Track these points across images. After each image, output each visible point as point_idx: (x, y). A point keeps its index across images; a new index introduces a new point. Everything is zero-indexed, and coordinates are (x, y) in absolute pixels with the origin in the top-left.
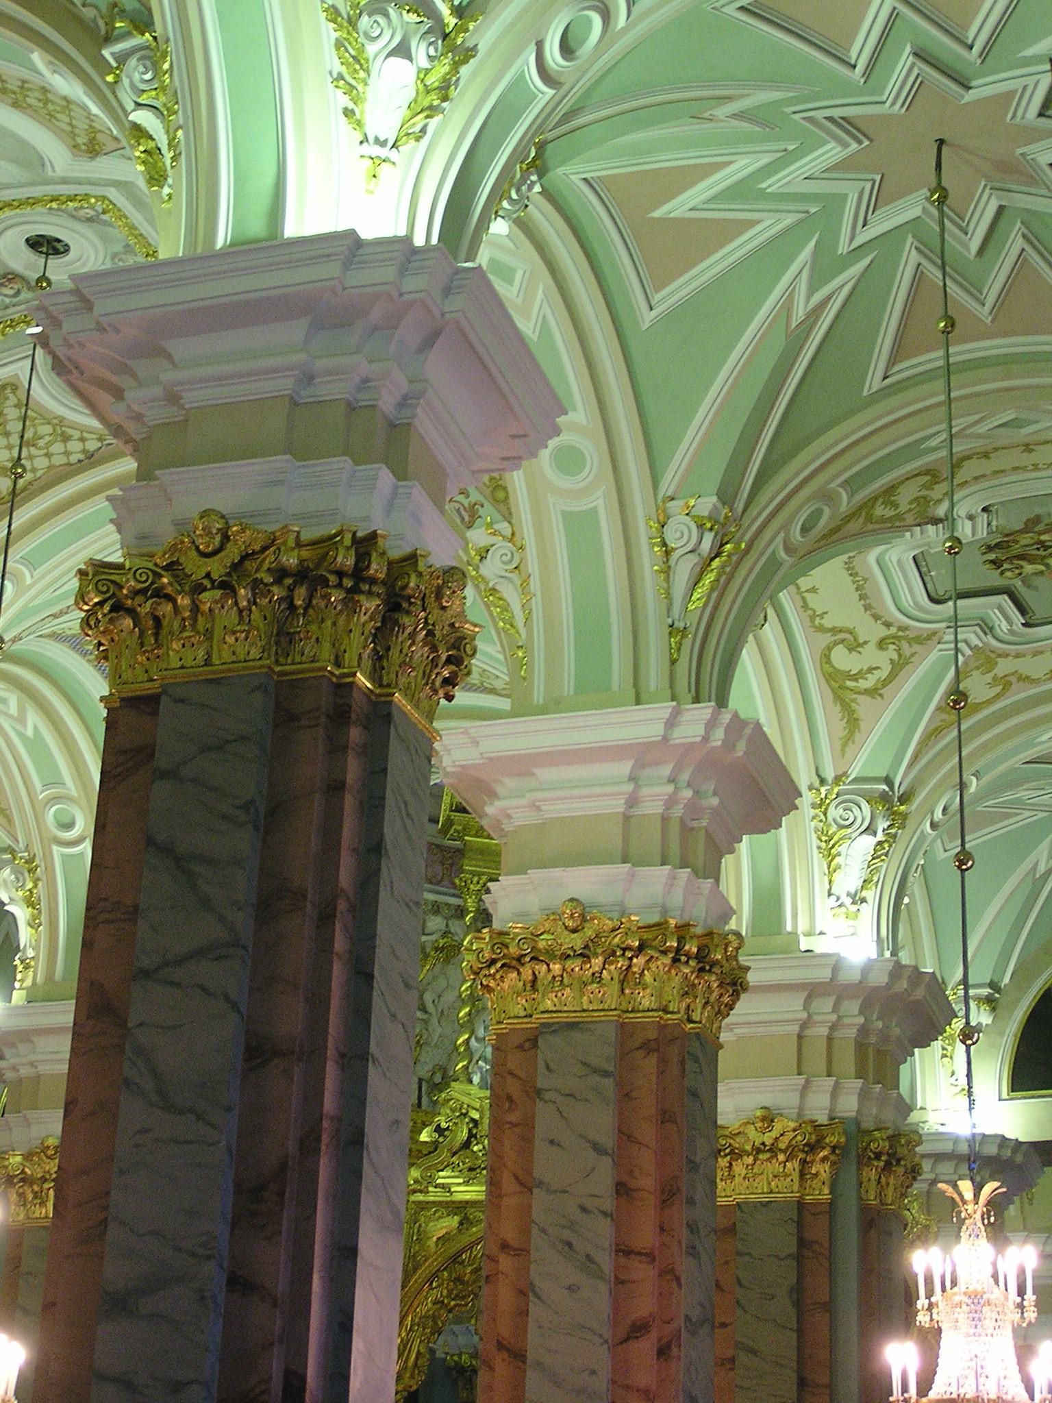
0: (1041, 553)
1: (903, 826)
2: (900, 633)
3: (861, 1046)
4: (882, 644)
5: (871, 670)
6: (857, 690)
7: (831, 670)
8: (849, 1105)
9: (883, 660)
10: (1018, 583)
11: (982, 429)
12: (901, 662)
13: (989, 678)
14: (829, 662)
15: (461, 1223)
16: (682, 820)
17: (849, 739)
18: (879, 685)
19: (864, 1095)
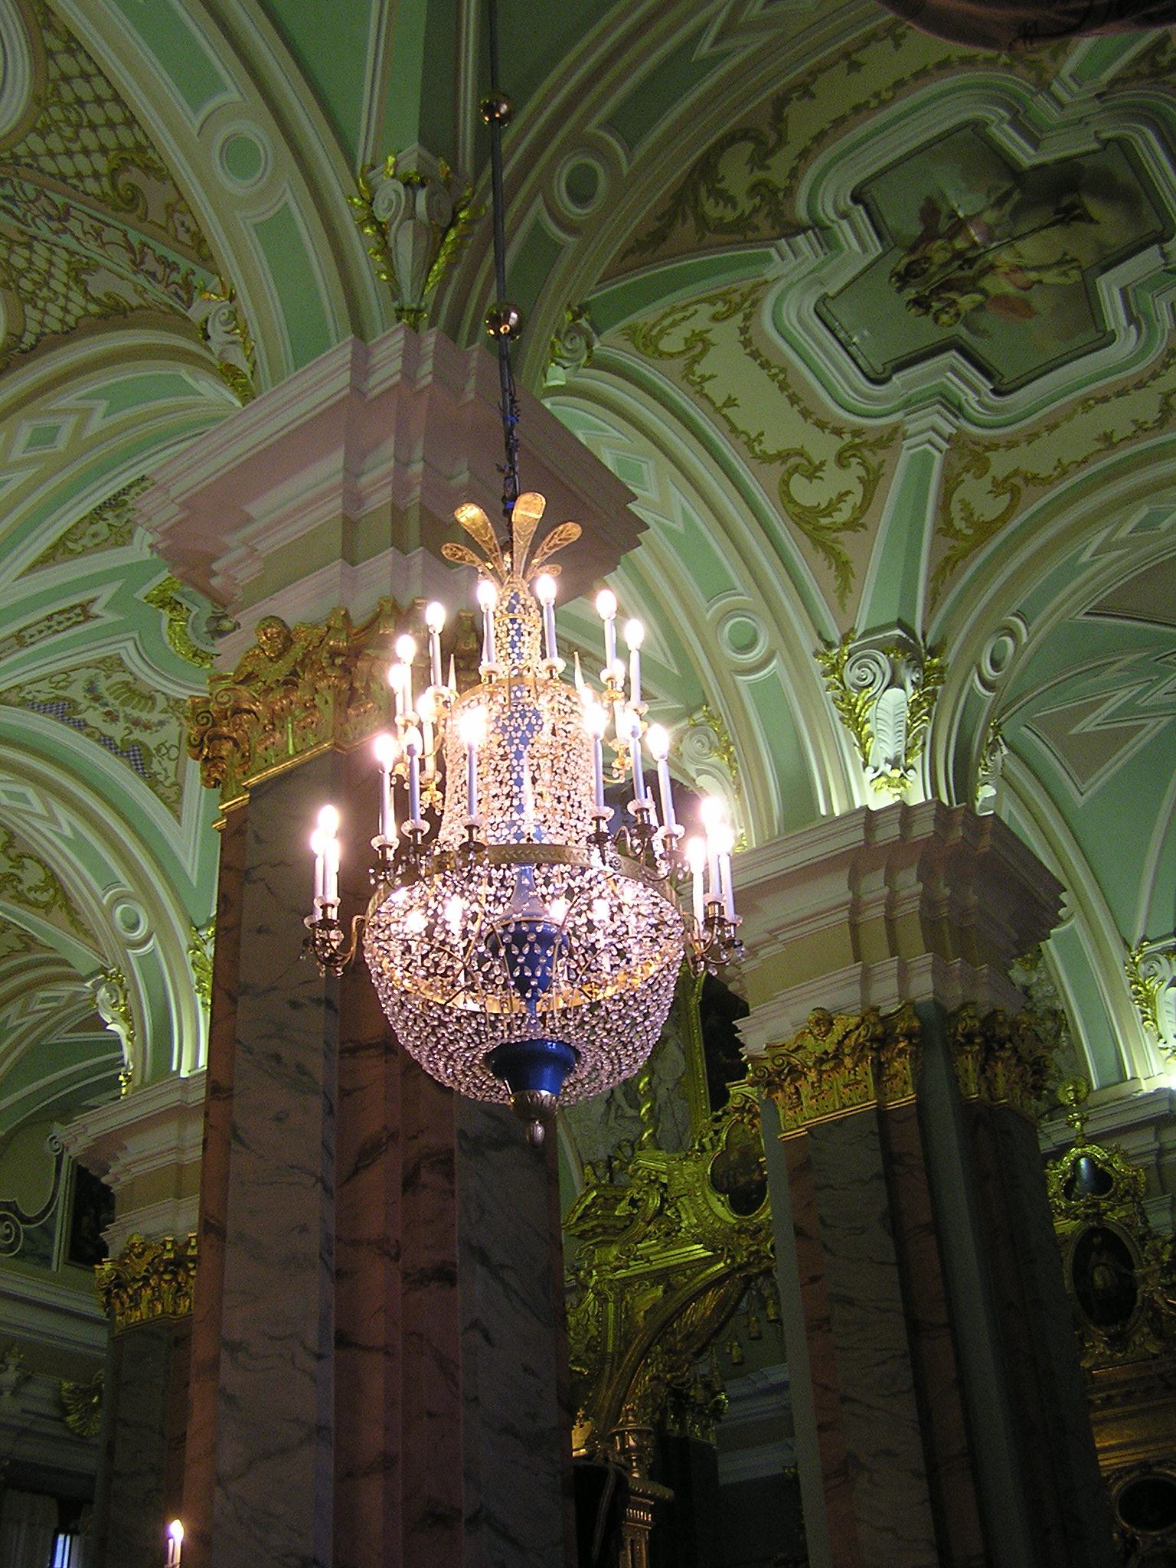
0: (968, 273)
1: (941, 680)
2: (857, 440)
3: (931, 926)
4: (841, 461)
5: (842, 496)
6: (835, 527)
7: (798, 510)
8: (923, 986)
9: (849, 479)
10: (963, 331)
11: (1123, 533)
12: (871, 477)
13: (986, 483)
14: (792, 501)
15: (665, 1292)
16: (423, 509)
17: (844, 589)
18: (857, 514)
19: (940, 973)
